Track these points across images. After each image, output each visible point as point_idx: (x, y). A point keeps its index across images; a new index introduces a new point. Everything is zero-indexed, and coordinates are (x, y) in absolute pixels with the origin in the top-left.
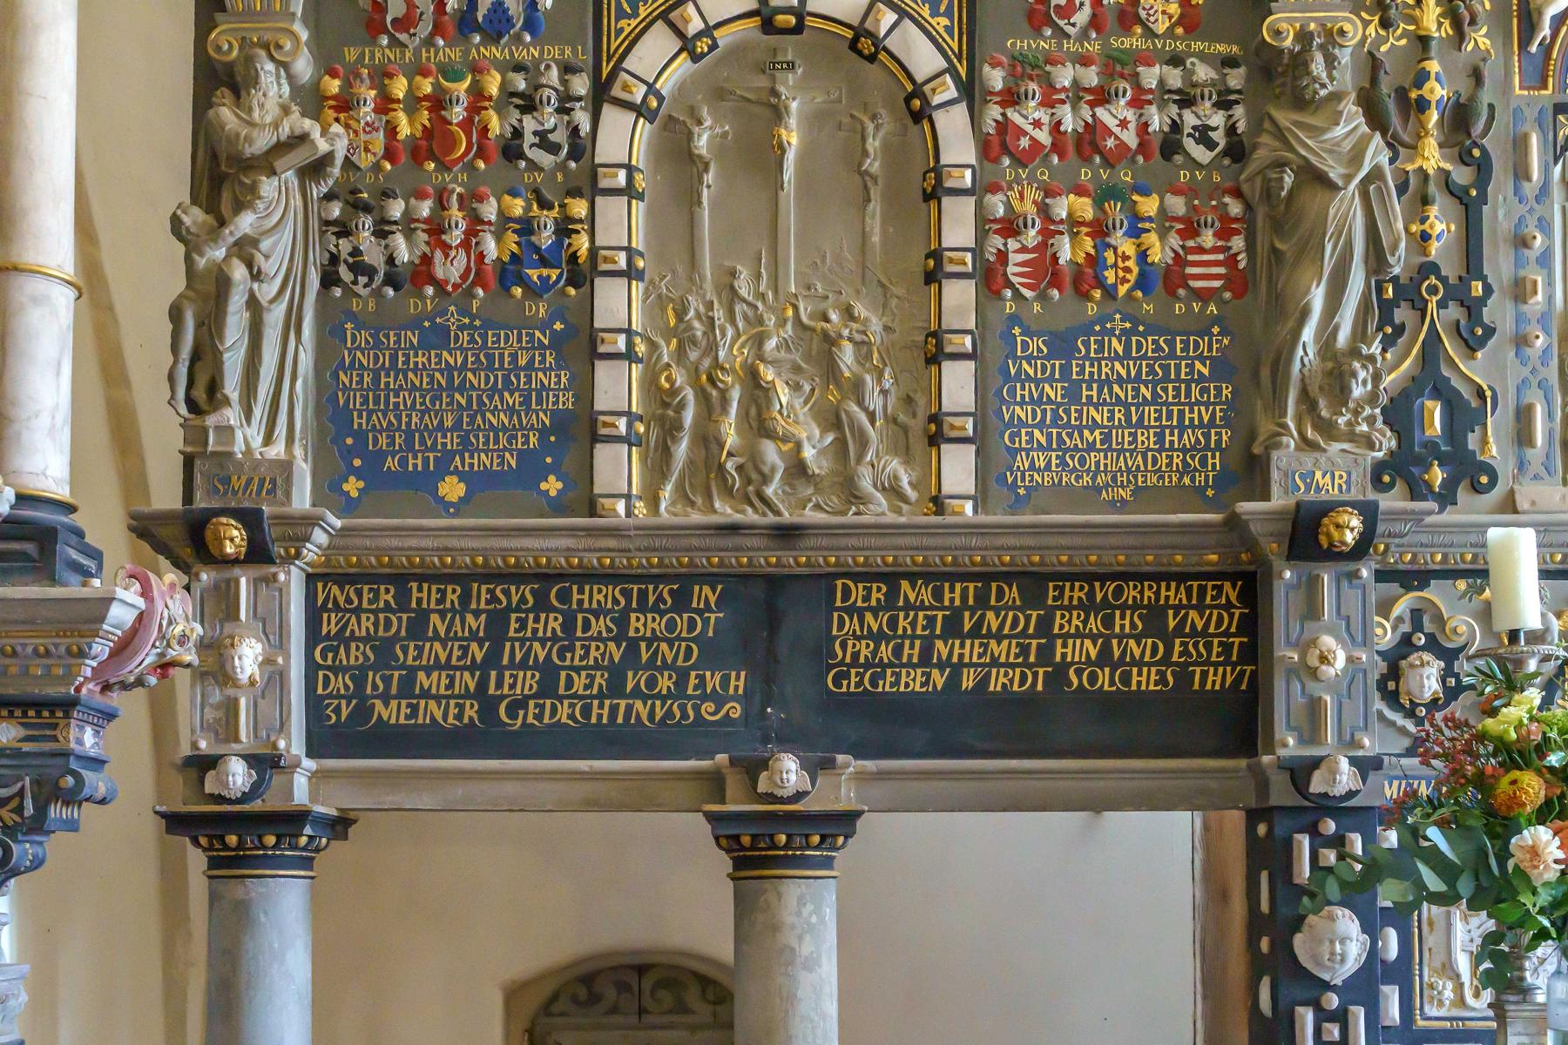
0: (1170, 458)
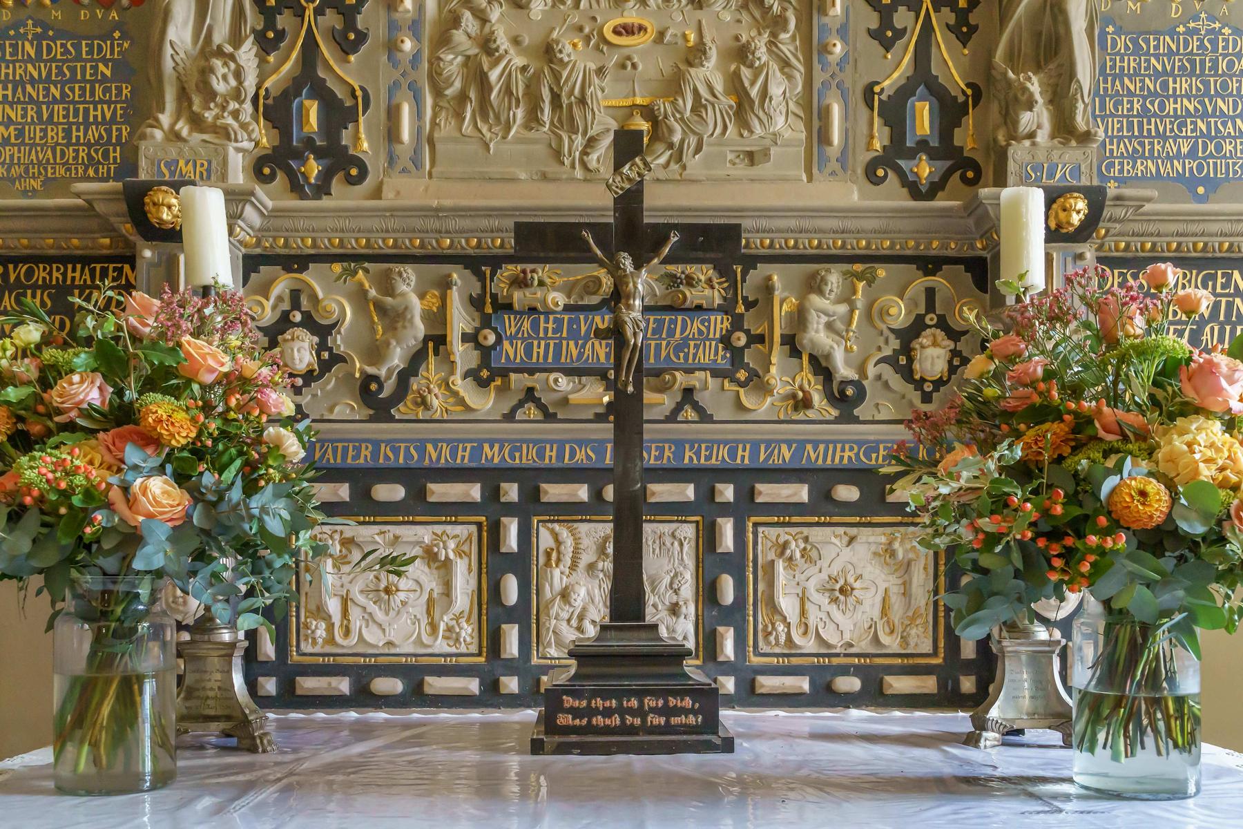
0: (76, 151)
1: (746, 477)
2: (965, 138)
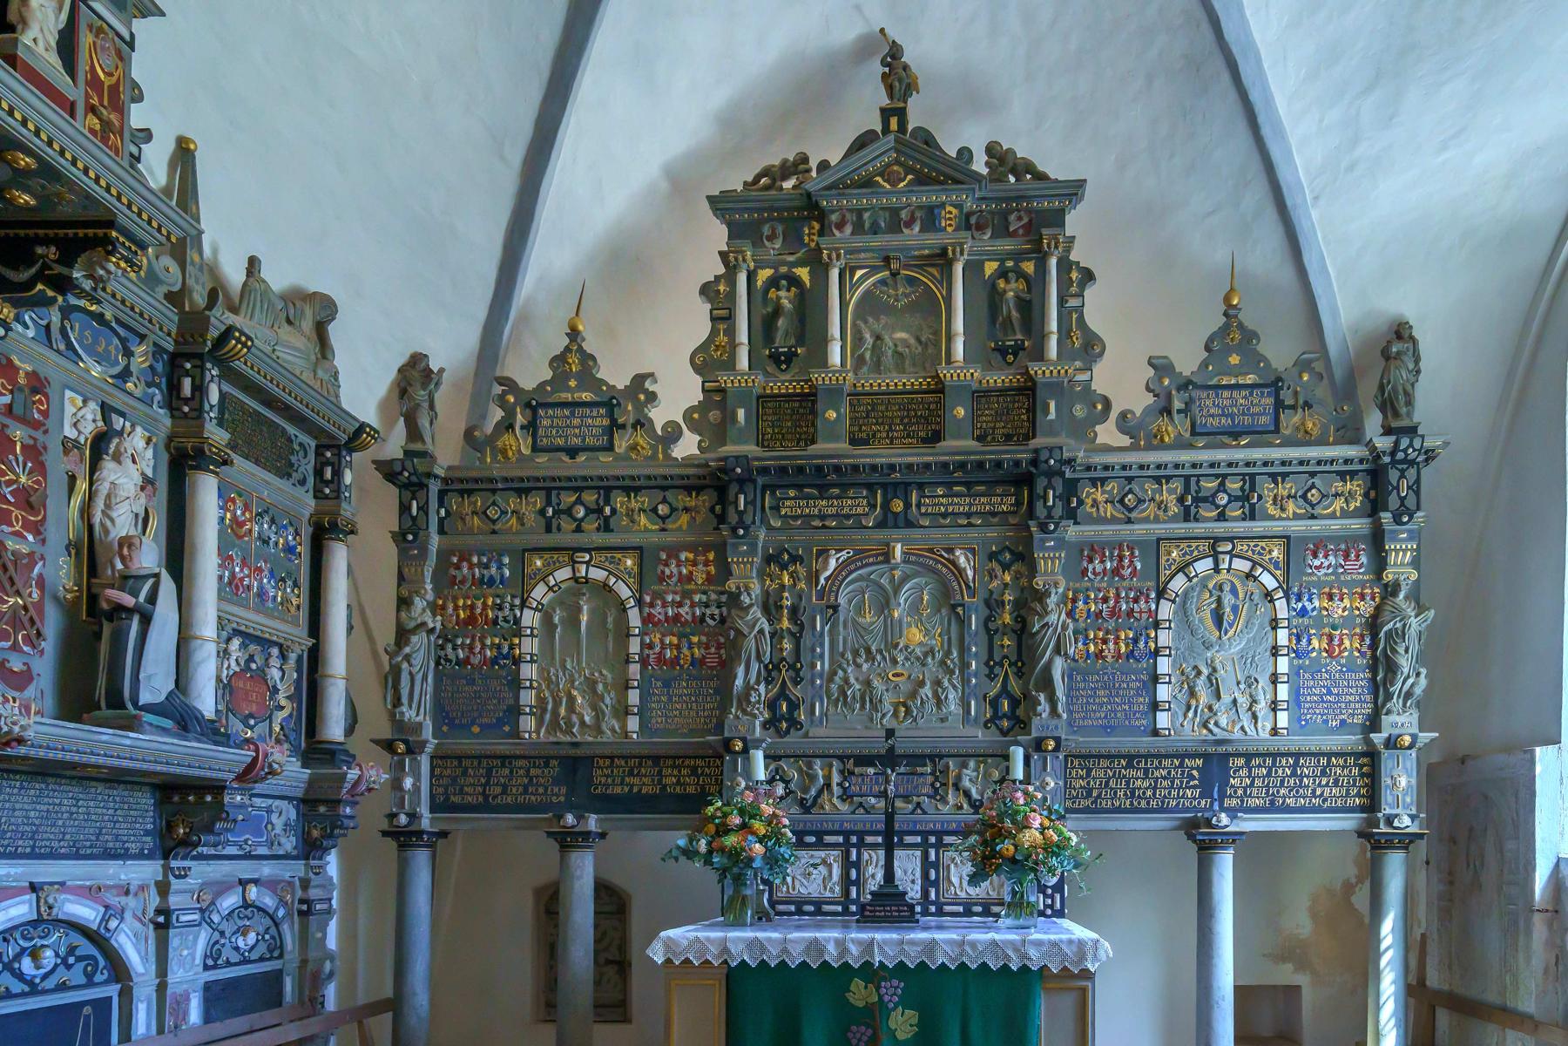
1: (940, 834)
2: (1020, 712)
